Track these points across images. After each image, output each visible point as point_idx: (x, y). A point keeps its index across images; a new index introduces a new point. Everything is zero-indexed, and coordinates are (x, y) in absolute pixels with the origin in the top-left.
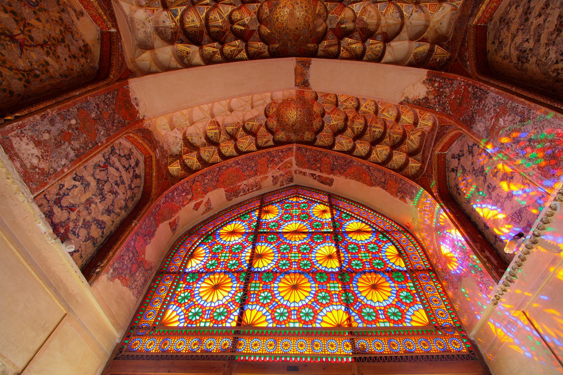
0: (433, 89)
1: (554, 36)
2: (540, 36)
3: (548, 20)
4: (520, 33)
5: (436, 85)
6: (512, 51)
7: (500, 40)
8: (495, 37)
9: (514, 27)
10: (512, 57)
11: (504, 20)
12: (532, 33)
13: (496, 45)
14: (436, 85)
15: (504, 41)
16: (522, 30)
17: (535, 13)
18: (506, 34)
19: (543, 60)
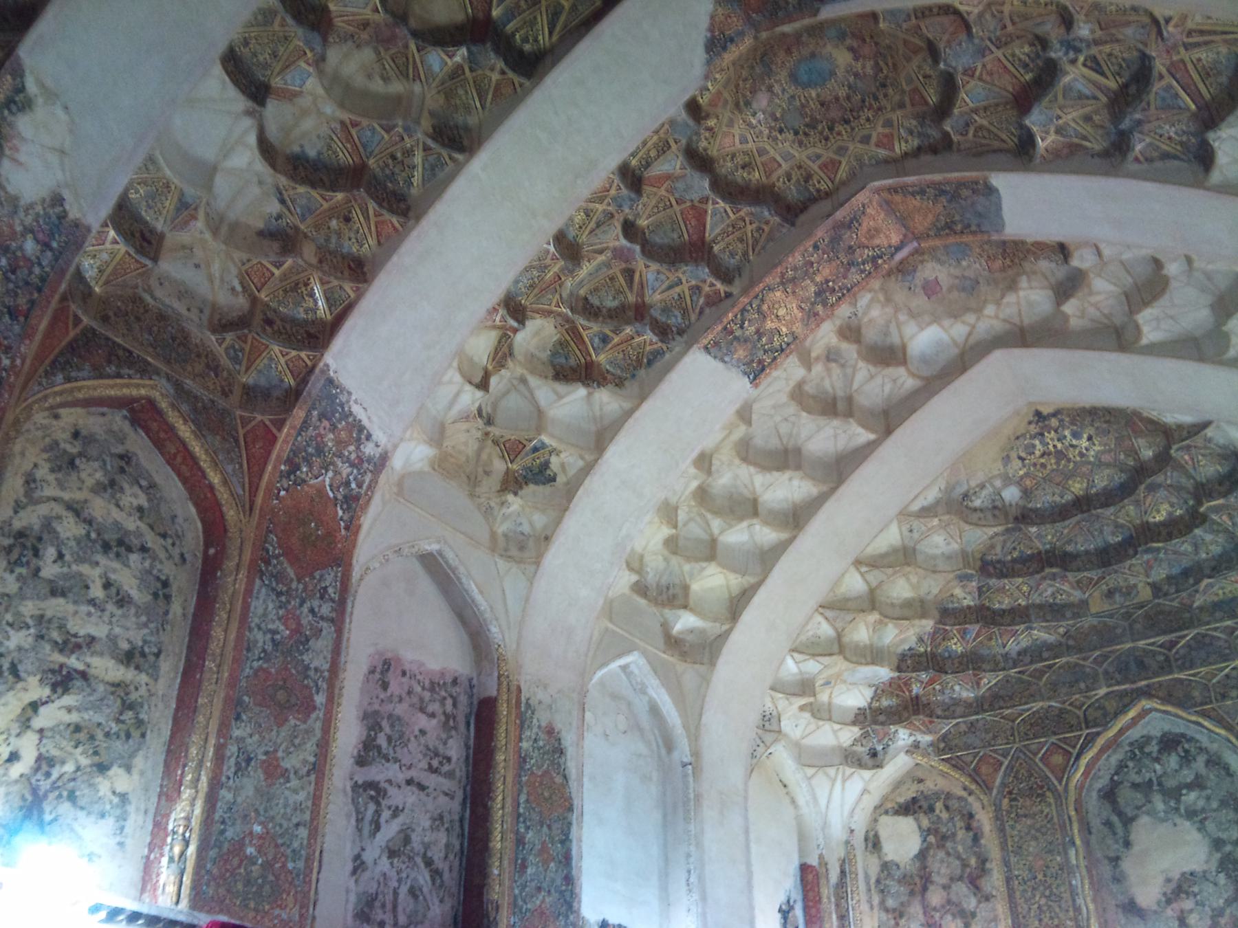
0: (19, 229)
1: (55, 635)
2: (63, 595)
3: (92, 610)
4: (78, 530)
5: (30, 246)
6: (43, 509)
7: (77, 462)
8: (90, 440)
9: (99, 508)
10: (30, 508)
11: (122, 470)
12: (74, 567)
13: (69, 448)
14: (30, 246)
15: (74, 476)
16: (88, 535)
17: (114, 571)
18: (90, 482)
19: (9, 617)
